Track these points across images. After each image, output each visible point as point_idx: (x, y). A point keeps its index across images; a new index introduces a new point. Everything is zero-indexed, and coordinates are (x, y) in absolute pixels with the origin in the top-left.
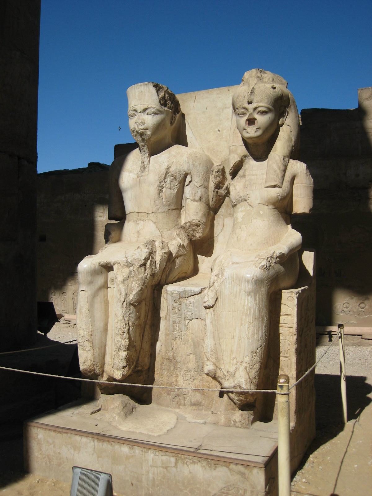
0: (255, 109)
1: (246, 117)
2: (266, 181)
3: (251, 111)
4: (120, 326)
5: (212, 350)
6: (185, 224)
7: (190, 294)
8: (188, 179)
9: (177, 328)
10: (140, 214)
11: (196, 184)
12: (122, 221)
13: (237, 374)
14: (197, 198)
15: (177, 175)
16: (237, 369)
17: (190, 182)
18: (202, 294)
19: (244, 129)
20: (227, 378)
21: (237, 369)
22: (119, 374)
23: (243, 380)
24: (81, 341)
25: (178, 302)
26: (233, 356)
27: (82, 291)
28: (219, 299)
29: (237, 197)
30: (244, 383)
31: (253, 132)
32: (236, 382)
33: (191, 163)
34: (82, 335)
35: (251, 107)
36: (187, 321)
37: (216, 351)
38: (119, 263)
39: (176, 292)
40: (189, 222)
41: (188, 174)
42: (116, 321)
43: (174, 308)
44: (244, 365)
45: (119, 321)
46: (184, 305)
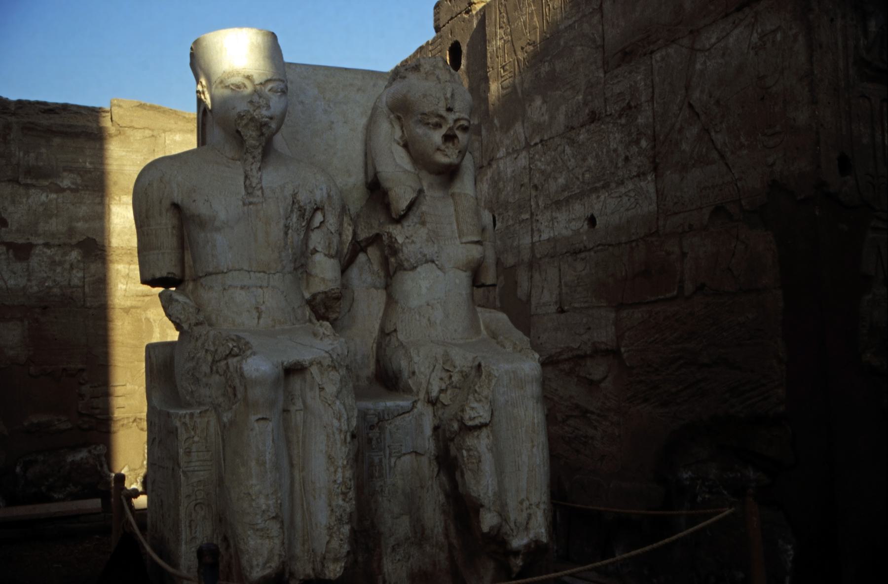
0: (456, 121)
1: (444, 130)
2: (461, 234)
3: (451, 123)
4: (343, 478)
5: (495, 494)
6: (314, 296)
7: (396, 414)
8: (319, 217)
9: (377, 474)
10: (252, 274)
11: (330, 227)
12: (181, 287)
13: (533, 523)
14: (333, 252)
15: (308, 208)
16: (529, 517)
17: (321, 223)
18: (415, 410)
19: (438, 149)
20: (515, 533)
21: (529, 517)
22: (338, 569)
23: (543, 530)
24: (260, 521)
25: (377, 429)
26: (523, 496)
27: (262, 422)
28: (496, 413)
29: (419, 256)
30: (544, 534)
31: (455, 157)
32: (531, 536)
33: (325, 191)
34: (264, 507)
35: (451, 117)
36: (393, 460)
37: (500, 494)
38: (320, 363)
39: (372, 412)
40: (325, 293)
41: (317, 209)
42: (332, 469)
43: (370, 440)
44: (542, 506)
45: (340, 470)
46: (387, 432)
